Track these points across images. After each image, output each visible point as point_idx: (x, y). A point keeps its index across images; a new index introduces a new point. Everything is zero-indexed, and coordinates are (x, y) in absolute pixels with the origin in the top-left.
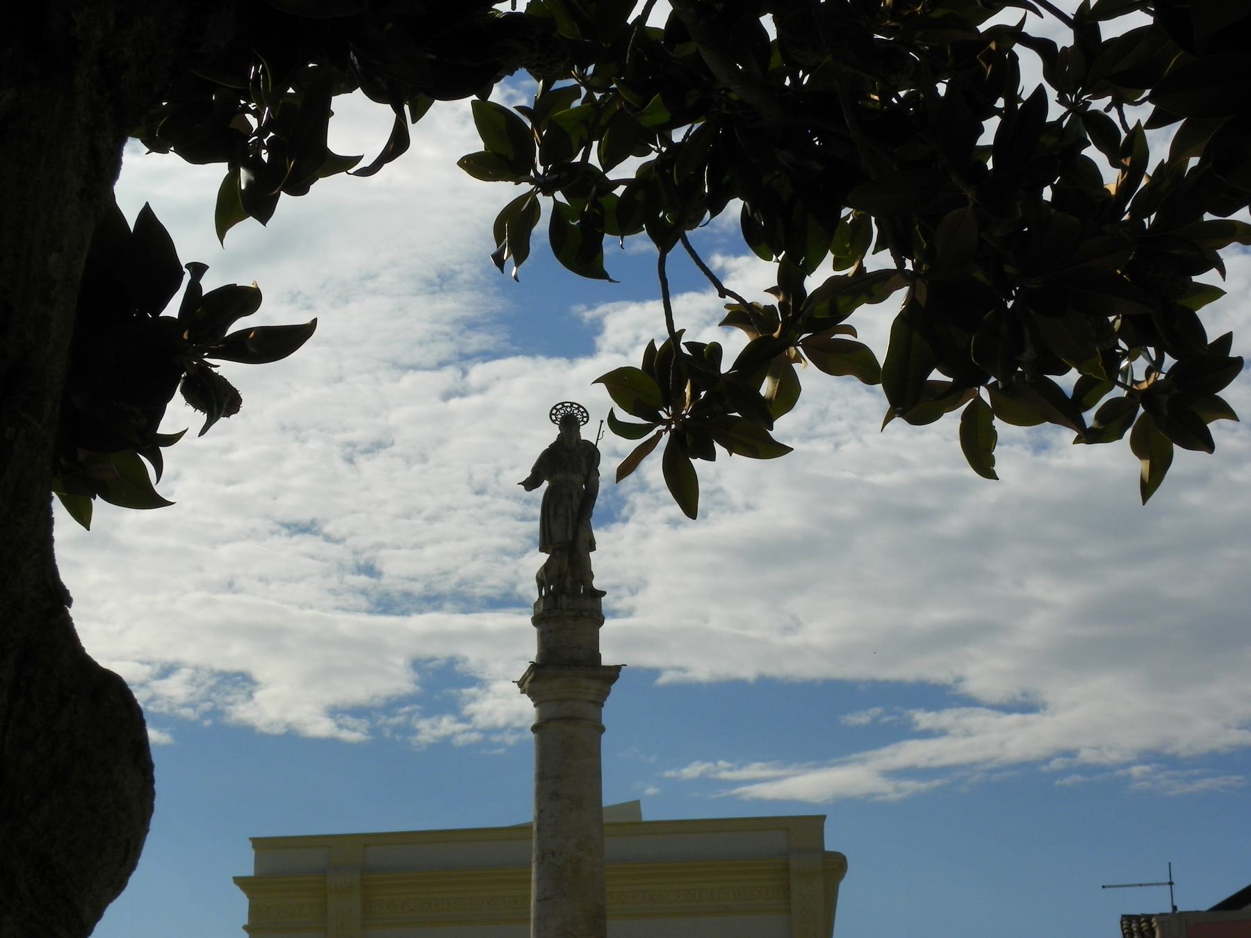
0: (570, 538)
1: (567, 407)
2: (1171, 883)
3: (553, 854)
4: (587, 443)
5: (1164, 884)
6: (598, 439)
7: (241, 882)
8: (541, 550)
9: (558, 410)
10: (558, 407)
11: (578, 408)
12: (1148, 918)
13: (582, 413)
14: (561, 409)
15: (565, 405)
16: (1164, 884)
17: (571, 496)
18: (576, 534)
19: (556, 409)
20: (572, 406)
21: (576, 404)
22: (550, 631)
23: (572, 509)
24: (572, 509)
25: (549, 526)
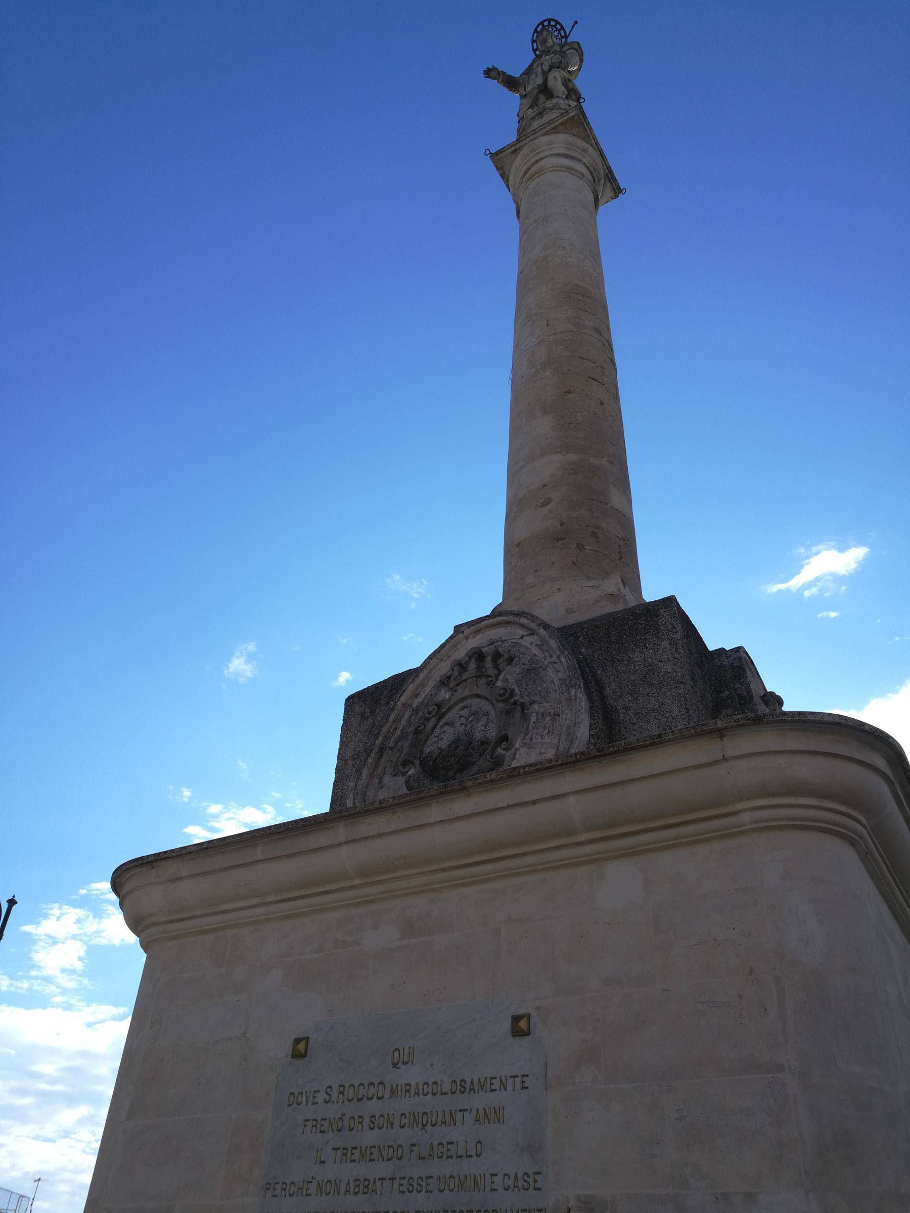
13: (562, 37)
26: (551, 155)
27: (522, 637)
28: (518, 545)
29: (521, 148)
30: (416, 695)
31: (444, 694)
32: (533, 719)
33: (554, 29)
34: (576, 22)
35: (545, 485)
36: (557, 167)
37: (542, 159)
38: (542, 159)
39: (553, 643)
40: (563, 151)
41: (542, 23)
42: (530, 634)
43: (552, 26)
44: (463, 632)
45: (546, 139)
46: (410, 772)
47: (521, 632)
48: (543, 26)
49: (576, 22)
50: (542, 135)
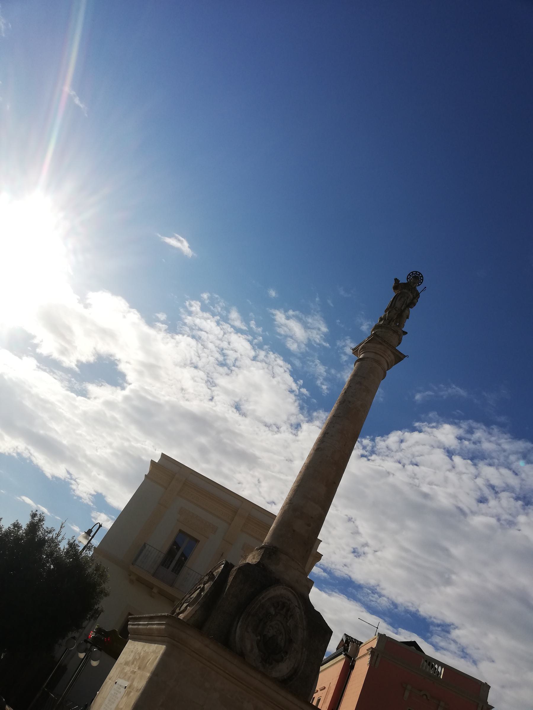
0: (403, 308)
2: (377, 628)
3: (350, 402)
5: (375, 627)
6: (422, 291)
9: (413, 274)
10: (414, 273)
11: (421, 277)
12: (352, 638)
14: (414, 274)
15: (417, 273)
16: (375, 627)
18: (405, 309)
19: (413, 273)
23: (407, 302)
24: (407, 302)
26: (386, 359)
28: (294, 531)
30: (263, 598)
31: (272, 611)
33: (420, 280)
35: (312, 517)
36: (383, 368)
37: (383, 357)
38: (383, 357)
40: (389, 361)
41: (420, 273)
42: (298, 608)
43: (421, 278)
44: (283, 586)
45: (389, 352)
46: (259, 638)
47: (297, 604)
48: (419, 275)
50: (390, 350)
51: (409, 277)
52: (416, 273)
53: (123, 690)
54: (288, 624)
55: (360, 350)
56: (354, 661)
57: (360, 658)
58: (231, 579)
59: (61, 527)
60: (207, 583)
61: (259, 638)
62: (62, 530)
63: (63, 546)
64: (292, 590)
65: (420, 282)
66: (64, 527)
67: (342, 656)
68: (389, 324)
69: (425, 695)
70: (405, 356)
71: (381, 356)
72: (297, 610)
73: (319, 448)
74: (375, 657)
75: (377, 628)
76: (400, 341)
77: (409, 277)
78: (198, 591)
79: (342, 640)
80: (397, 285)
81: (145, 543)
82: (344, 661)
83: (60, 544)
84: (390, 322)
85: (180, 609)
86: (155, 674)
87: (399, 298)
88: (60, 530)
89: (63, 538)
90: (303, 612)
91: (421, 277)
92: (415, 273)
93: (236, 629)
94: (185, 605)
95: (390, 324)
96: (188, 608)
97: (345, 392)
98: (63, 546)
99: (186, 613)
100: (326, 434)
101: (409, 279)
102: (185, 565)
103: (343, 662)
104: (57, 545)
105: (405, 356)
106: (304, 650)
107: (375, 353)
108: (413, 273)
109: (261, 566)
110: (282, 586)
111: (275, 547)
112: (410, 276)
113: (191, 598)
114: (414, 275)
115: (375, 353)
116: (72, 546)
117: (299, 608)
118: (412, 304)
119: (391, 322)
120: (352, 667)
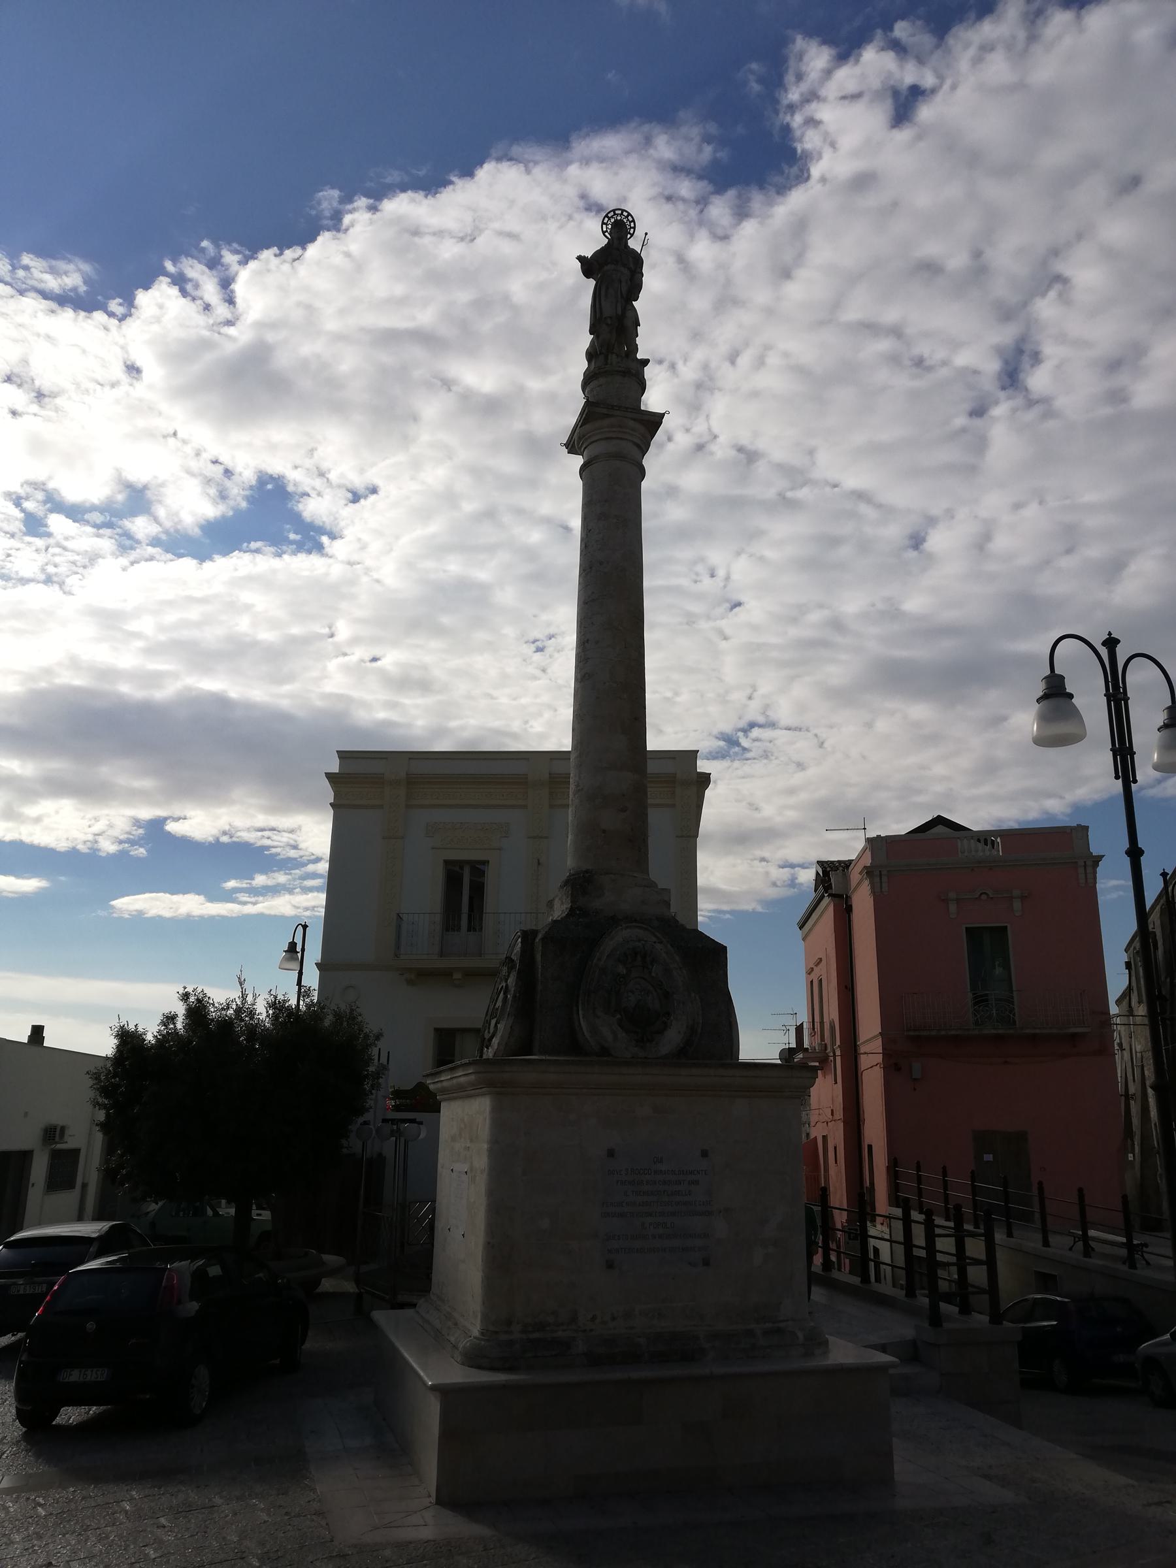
0: (620, 312)
1: (618, 215)
2: (865, 829)
3: (601, 563)
4: (634, 251)
6: (643, 245)
7: (329, 776)
8: (591, 334)
9: (609, 219)
10: (610, 215)
11: (627, 217)
14: (612, 217)
17: (620, 282)
18: (624, 310)
19: (608, 217)
20: (622, 214)
21: (626, 211)
22: (600, 386)
25: (600, 304)
26: (630, 440)
27: (655, 942)
28: (604, 831)
29: (612, 416)
31: (622, 970)
32: (676, 1004)
34: (646, 234)
35: (624, 795)
39: (677, 958)
42: (659, 943)
43: (628, 220)
45: (631, 423)
46: (619, 1016)
47: (654, 939)
49: (646, 234)
50: (632, 419)
51: (604, 229)
52: (615, 214)
53: (465, 1177)
54: (653, 974)
55: (578, 444)
56: (848, 898)
57: (855, 889)
58: (538, 957)
59: (241, 984)
60: (508, 976)
61: (618, 1016)
62: (245, 986)
63: (262, 1010)
64: (637, 924)
65: (631, 228)
66: (245, 980)
67: (826, 900)
68: (606, 364)
69: (981, 894)
70: (663, 415)
71: (621, 439)
72: (658, 946)
73: (585, 674)
74: (877, 880)
75: (865, 829)
76: (643, 383)
77: (604, 229)
78: (502, 993)
79: (817, 873)
80: (589, 266)
81: (398, 914)
82: (832, 906)
83: (255, 1007)
84: (606, 358)
85: (489, 1032)
86: (494, 1141)
87: (603, 293)
88: (242, 989)
89: (255, 997)
90: (669, 946)
91: (627, 217)
92: (612, 213)
93: (580, 1024)
94: (493, 1022)
95: (609, 361)
96: (499, 1025)
97: (586, 546)
98: (262, 1010)
99: (499, 1035)
100: (586, 644)
101: (607, 231)
102: (484, 911)
103: (831, 909)
104: (252, 1014)
105: (663, 415)
106: (693, 995)
107: (607, 439)
108: (608, 217)
109: (578, 912)
110: (620, 927)
111: (587, 871)
112: (606, 224)
113: (497, 1009)
114: (613, 220)
115: (607, 439)
116: (277, 1006)
117: (661, 942)
118: (635, 288)
119: (609, 358)
120: (849, 909)
